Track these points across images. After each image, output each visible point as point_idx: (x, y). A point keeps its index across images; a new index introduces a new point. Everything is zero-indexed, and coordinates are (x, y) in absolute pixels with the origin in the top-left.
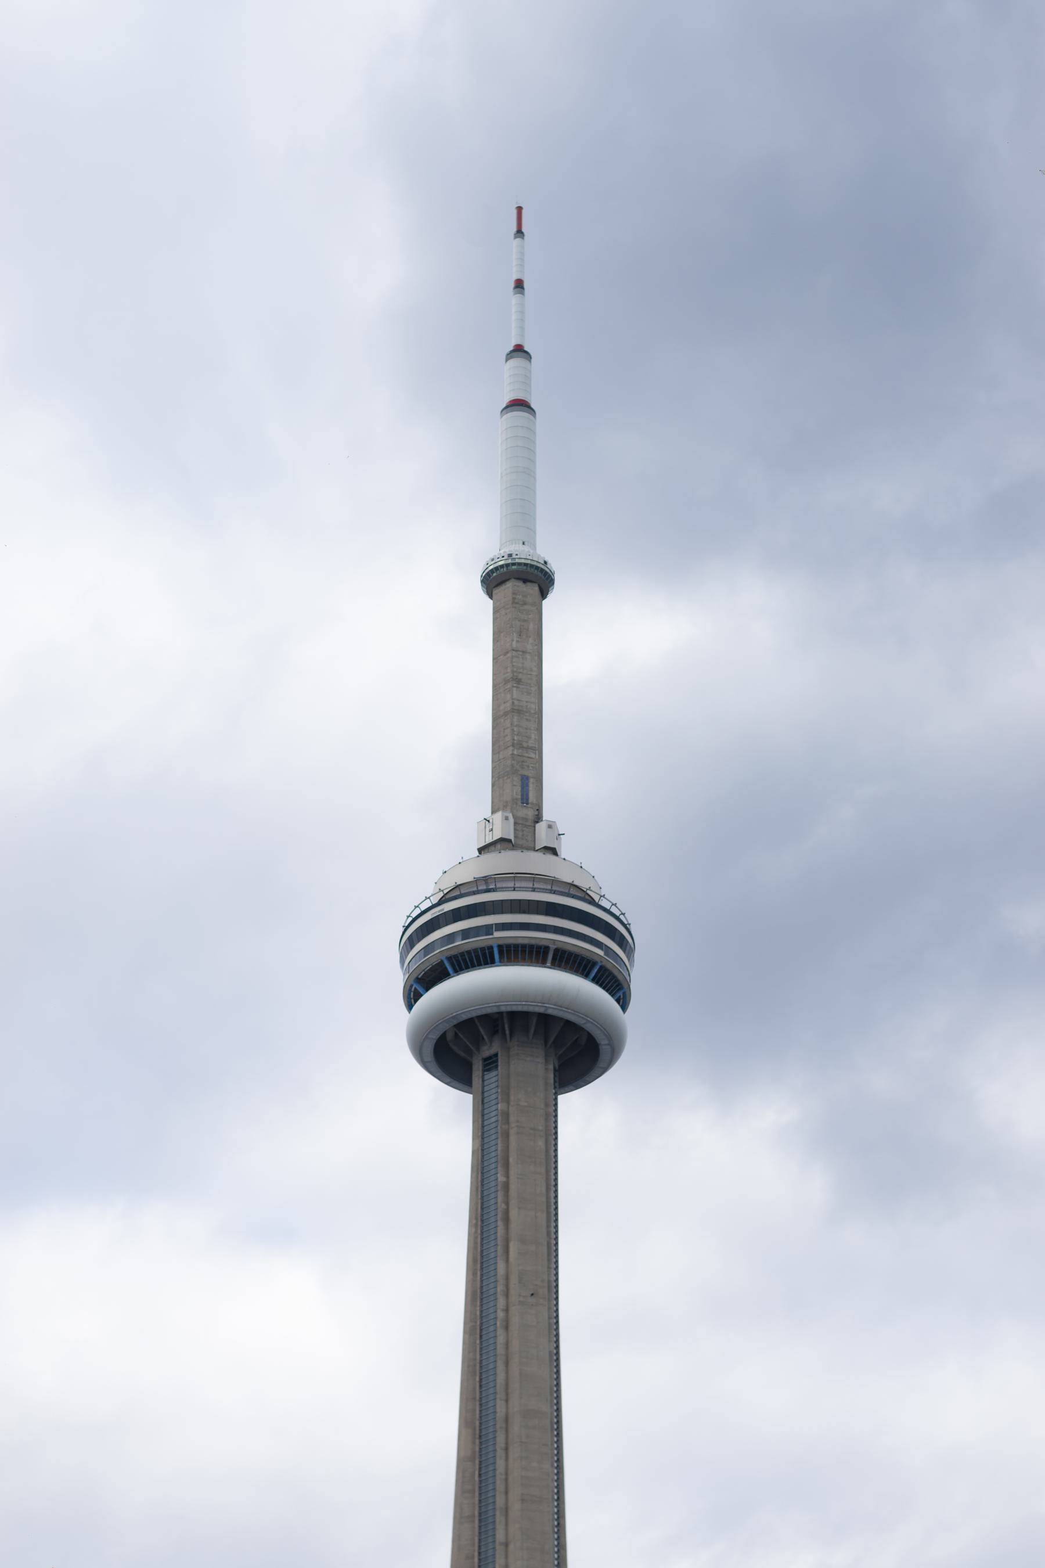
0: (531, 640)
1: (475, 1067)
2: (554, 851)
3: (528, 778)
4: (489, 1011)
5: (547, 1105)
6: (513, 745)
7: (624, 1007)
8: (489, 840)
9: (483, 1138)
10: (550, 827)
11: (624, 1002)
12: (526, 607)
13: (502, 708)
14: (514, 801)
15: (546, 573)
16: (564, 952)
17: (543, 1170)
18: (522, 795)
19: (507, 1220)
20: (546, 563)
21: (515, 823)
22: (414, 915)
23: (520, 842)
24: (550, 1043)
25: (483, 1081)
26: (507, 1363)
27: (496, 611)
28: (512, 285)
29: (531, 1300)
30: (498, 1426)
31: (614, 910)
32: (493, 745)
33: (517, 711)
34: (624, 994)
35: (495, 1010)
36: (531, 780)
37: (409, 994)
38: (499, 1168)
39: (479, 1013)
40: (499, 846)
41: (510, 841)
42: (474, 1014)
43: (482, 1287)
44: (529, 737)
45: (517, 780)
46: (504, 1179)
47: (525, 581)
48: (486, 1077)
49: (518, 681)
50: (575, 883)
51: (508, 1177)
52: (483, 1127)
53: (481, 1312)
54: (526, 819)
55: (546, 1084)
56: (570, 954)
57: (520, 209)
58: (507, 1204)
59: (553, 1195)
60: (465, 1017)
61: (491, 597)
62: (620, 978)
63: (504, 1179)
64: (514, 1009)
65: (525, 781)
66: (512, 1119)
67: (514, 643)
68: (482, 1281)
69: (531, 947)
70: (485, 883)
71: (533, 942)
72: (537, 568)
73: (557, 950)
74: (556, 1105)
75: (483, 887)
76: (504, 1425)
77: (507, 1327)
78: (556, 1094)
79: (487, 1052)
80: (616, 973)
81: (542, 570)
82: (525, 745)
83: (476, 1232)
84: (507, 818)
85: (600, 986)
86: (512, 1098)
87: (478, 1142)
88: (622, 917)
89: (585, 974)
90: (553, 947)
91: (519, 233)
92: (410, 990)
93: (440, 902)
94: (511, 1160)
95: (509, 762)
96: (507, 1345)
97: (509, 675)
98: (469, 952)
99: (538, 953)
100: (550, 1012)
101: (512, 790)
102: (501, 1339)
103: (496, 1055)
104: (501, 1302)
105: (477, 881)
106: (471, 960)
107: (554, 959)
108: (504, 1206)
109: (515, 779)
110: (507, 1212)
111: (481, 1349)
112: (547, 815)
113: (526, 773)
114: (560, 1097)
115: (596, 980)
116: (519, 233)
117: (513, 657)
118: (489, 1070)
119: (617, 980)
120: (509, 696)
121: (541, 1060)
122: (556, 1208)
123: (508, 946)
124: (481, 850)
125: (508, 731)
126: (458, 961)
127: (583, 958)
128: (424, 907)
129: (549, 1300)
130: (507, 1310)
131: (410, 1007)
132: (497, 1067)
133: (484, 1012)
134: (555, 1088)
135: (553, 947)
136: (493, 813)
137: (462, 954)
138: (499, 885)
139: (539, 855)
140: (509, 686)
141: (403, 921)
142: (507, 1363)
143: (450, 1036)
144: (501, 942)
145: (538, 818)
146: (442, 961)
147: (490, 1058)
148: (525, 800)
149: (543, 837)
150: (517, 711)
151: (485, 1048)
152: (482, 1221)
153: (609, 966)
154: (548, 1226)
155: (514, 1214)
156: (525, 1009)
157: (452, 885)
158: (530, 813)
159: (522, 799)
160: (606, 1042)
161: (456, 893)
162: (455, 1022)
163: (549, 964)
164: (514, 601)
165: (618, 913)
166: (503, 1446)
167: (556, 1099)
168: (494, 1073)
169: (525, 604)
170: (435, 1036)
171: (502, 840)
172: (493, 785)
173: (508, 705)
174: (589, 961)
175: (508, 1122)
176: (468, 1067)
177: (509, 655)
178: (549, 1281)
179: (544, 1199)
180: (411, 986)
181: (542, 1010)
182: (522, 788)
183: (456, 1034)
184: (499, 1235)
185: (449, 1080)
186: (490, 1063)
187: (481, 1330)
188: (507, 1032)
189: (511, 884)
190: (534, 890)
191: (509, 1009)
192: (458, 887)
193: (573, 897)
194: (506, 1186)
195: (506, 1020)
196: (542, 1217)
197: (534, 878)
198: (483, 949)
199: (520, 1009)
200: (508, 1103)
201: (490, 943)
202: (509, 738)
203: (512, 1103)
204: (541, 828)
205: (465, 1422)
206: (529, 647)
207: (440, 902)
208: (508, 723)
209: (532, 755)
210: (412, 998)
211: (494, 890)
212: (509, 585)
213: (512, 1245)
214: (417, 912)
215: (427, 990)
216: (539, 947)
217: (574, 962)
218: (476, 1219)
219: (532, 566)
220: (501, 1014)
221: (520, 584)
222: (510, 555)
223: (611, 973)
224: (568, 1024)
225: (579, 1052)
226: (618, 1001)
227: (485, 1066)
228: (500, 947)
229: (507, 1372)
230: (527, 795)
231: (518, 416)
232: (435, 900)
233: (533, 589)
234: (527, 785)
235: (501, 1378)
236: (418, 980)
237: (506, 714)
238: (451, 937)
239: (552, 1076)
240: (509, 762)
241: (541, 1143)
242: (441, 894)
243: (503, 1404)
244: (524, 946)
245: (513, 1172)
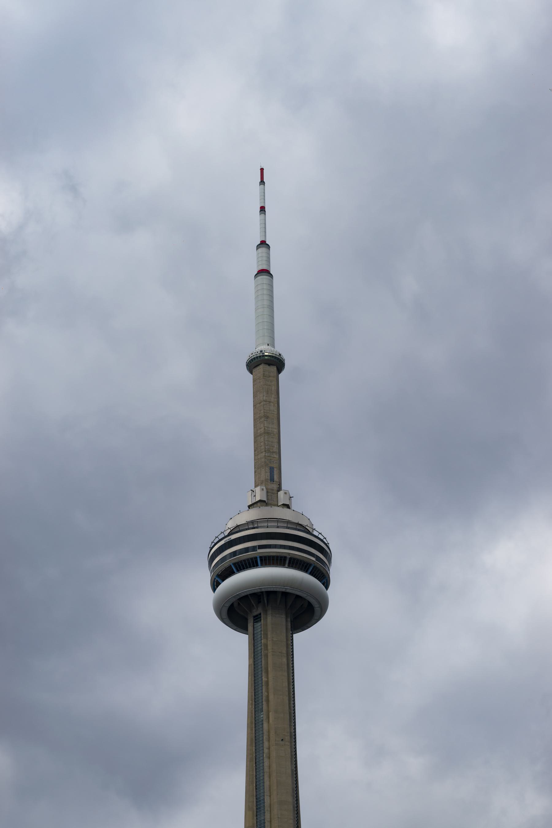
0: (273, 396)
1: (249, 621)
2: (288, 506)
3: (273, 468)
4: (256, 591)
5: (287, 640)
7: (327, 587)
8: (254, 501)
9: (254, 658)
10: (285, 493)
11: (327, 585)
12: (270, 378)
14: (266, 480)
15: (281, 360)
16: (294, 559)
17: (286, 674)
18: (271, 477)
19: (268, 701)
20: (280, 355)
21: (267, 492)
22: (215, 542)
23: (270, 502)
25: (254, 628)
26: (270, 777)
27: (254, 381)
28: (259, 210)
29: (281, 743)
30: (266, 809)
31: (320, 536)
32: (255, 451)
33: (267, 433)
34: (327, 580)
35: (259, 591)
36: (275, 469)
37: (214, 583)
38: (263, 674)
39: (251, 592)
40: (259, 504)
41: (264, 501)
42: (248, 593)
43: (255, 737)
44: (274, 447)
45: (268, 470)
46: (266, 679)
47: (269, 365)
48: (255, 626)
49: (267, 417)
50: (300, 523)
51: (268, 678)
52: (254, 652)
53: (256, 749)
54: (273, 490)
55: (287, 629)
56: (298, 560)
57: (262, 170)
58: (268, 693)
59: (292, 687)
60: (243, 595)
61: (252, 373)
62: (324, 572)
63: (266, 679)
64: (269, 590)
65: (272, 470)
66: (269, 647)
67: (265, 397)
68: (255, 733)
69: (277, 557)
70: (252, 524)
71: (278, 554)
72: (276, 357)
73: (290, 559)
74: (292, 639)
75: (251, 526)
76: (269, 809)
77: (269, 758)
78: (292, 634)
79: (255, 613)
80: (322, 569)
81: (278, 359)
82: (271, 451)
83: (252, 707)
84: (263, 490)
85: (314, 576)
86: (269, 636)
87: (252, 660)
88: (324, 540)
89: (306, 571)
90: (288, 557)
91: (262, 182)
92: (214, 581)
93: (230, 534)
94: (269, 669)
95: (263, 460)
96: (270, 767)
98: (244, 560)
99: (281, 560)
100: (288, 591)
101: (265, 474)
102: (266, 764)
103: (260, 614)
104: (266, 744)
105: (248, 523)
106: (246, 565)
107: (289, 563)
108: (266, 694)
109: (267, 469)
110: (268, 697)
111: (256, 769)
112: (284, 487)
113: (272, 466)
114: (294, 635)
115: (311, 574)
116: (262, 182)
117: (264, 405)
118: (256, 622)
119: (323, 573)
120: (262, 425)
121: (284, 616)
122: (294, 694)
123: (265, 557)
124: (249, 507)
125: (262, 444)
126: (239, 565)
127: (304, 562)
128: (220, 537)
129: (291, 743)
130: (269, 748)
131: (214, 590)
132: (261, 620)
133: (253, 592)
134: (291, 631)
135: (288, 557)
136: (255, 487)
137: (241, 562)
138: (259, 525)
139: (280, 509)
140: (263, 419)
141: (209, 545)
142: (270, 777)
143: (236, 605)
144: (261, 555)
145: (279, 489)
146: (231, 565)
147: (257, 616)
148: (272, 480)
149: (282, 498)
150: (267, 433)
151: (254, 610)
152: (255, 702)
153: (318, 566)
154: (290, 704)
155: (271, 697)
156: (275, 590)
157: (235, 525)
158: (275, 487)
159: (271, 479)
161: (237, 529)
162: (238, 597)
163: (287, 566)
164: (264, 376)
165: (322, 538)
166: (269, 820)
167: (292, 637)
168: (259, 624)
169: (270, 377)
170: (228, 605)
171: (260, 501)
172: (255, 472)
173: (262, 430)
174: (308, 564)
175: (267, 650)
176: (246, 620)
178: (291, 732)
179: (287, 689)
180: (215, 579)
181: (284, 590)
182: (271, 474)
183: (239, 604)
185: (235, 628)
186: (257, 618)
187: (256, 759)
188: (266, 602)
189: (266, 524)
190: (278, 527)
191: (266, 590)
192: (238, 526)
193: (299, 530)
194: (267, 683)
195: (265, 596)
196: (286, 698)
197: (278, 520)
198: (252, 559)
199: (272, 590)
200: (267, 639)
201: (255, 556)
202: (263, 447)
203: (269, 639)
204: (281, 494)
205: (248, 808)
206: (272, 400)
207: (230, 534)
208: (262, 439)
209: (276, 456)
210: (215, 585)
211: (257, 528)
212: (261, 367)
213: (271, 714)
214: (217, 540)
215: (223, 581)
216: (281, 557)
217: (300, 564)
218: (252, 701)
219: (272, 357)
220: (262, 592)
221: (267, 366)
222: (261, 351)
223: (319, 570)
224: (298, 597)
225: (304, 610)
226: (323, 584)
227: (254, 620)
228: (261, 557)
229: (270, 781)
230: (273, 477)
231: (264, 278)
232: (226, 533)
233: (274, 369)
234: (273, 472)
235: (267, 784)
236: (218, 576)
237: (261, 435)
238: (234, 554)
239: (289, 624)
240: (263, 460)
241: (285, 660)
242: (229, 530)
243: (269, 797)
244: (273, 557)
245: (271, 676)
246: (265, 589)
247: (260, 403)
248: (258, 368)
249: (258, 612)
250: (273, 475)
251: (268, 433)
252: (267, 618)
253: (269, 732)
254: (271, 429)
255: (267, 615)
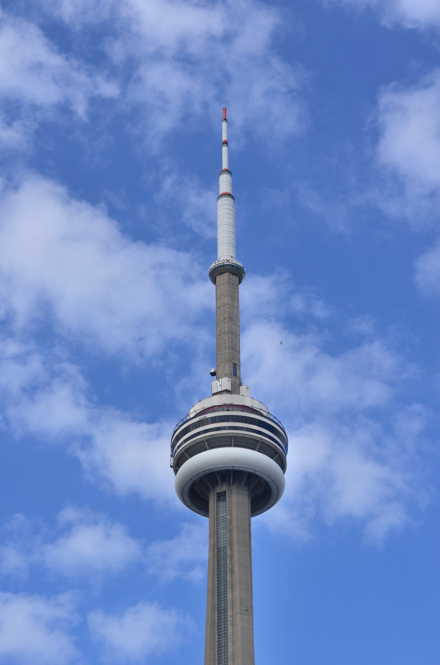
3: (236, 364)
6: (229, 348)
7: (284, 472)
13: (223, 330)
18: (234, 372)
24: (250, 490)
26: (233, 643)
29: (245, 612)
45: (232, 365)
46: (231, 552)
47: (233, 274)
63: (231, 552)
65: (235, 366)
67: (229, 301)
95: (228, 356)
97: (227, 316)
102: (230, 630)
104: (230, 613)
108: (230, 566)
117: (229, 308)
120: (226, 325)
140: (227, 320)
160: (276, 494)
164: (229, 282)
173: (227, 330)
177: (227, 306)
182: (234, 369)
184: (228, 579)
186: (221, 496)
203: (234, 516)
221: (231, 275)
229: (233, 648)
234: (236, 368)
235: (230, 650)
237: (225, 333)
240: (228, 356)
243: (232, 663)
246: (228, 466)
247: (224, 306)
248: (222, 276)
249: (223, 490)
250: (236, 370)
251: (232, 333)
252: (231, 496)
253: (232, 600)
254: (234, 330)
255: (231, 494)
